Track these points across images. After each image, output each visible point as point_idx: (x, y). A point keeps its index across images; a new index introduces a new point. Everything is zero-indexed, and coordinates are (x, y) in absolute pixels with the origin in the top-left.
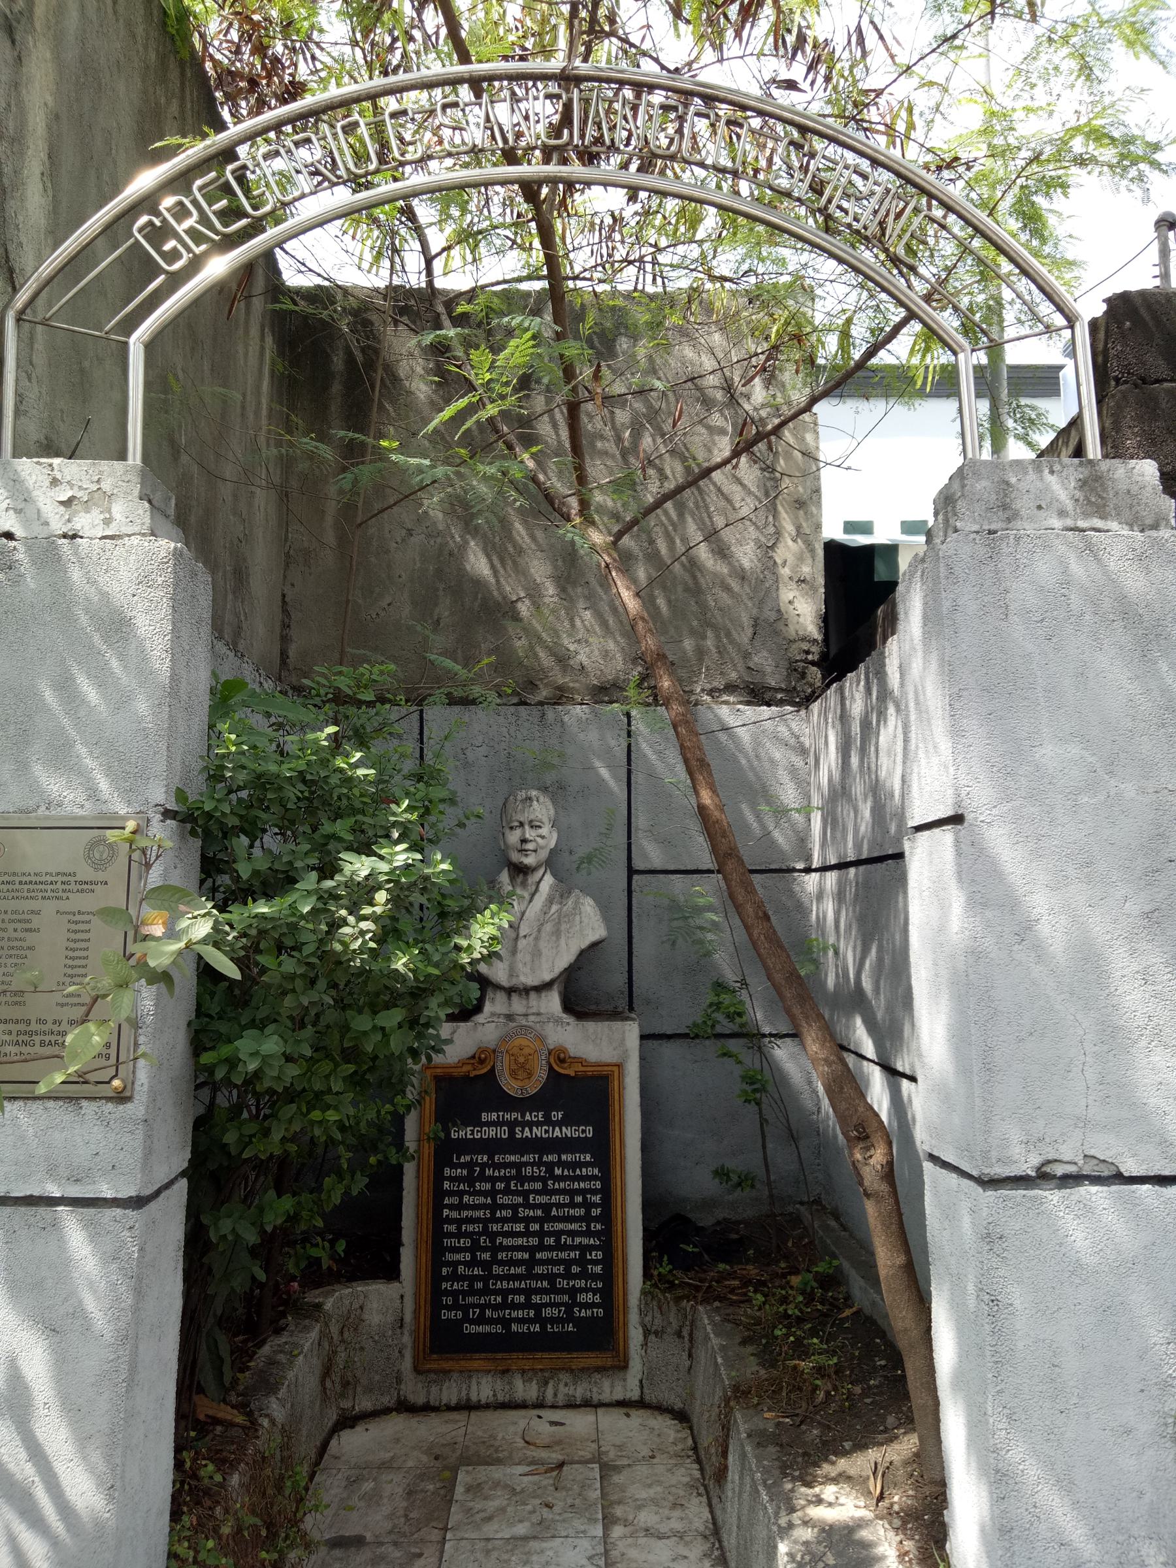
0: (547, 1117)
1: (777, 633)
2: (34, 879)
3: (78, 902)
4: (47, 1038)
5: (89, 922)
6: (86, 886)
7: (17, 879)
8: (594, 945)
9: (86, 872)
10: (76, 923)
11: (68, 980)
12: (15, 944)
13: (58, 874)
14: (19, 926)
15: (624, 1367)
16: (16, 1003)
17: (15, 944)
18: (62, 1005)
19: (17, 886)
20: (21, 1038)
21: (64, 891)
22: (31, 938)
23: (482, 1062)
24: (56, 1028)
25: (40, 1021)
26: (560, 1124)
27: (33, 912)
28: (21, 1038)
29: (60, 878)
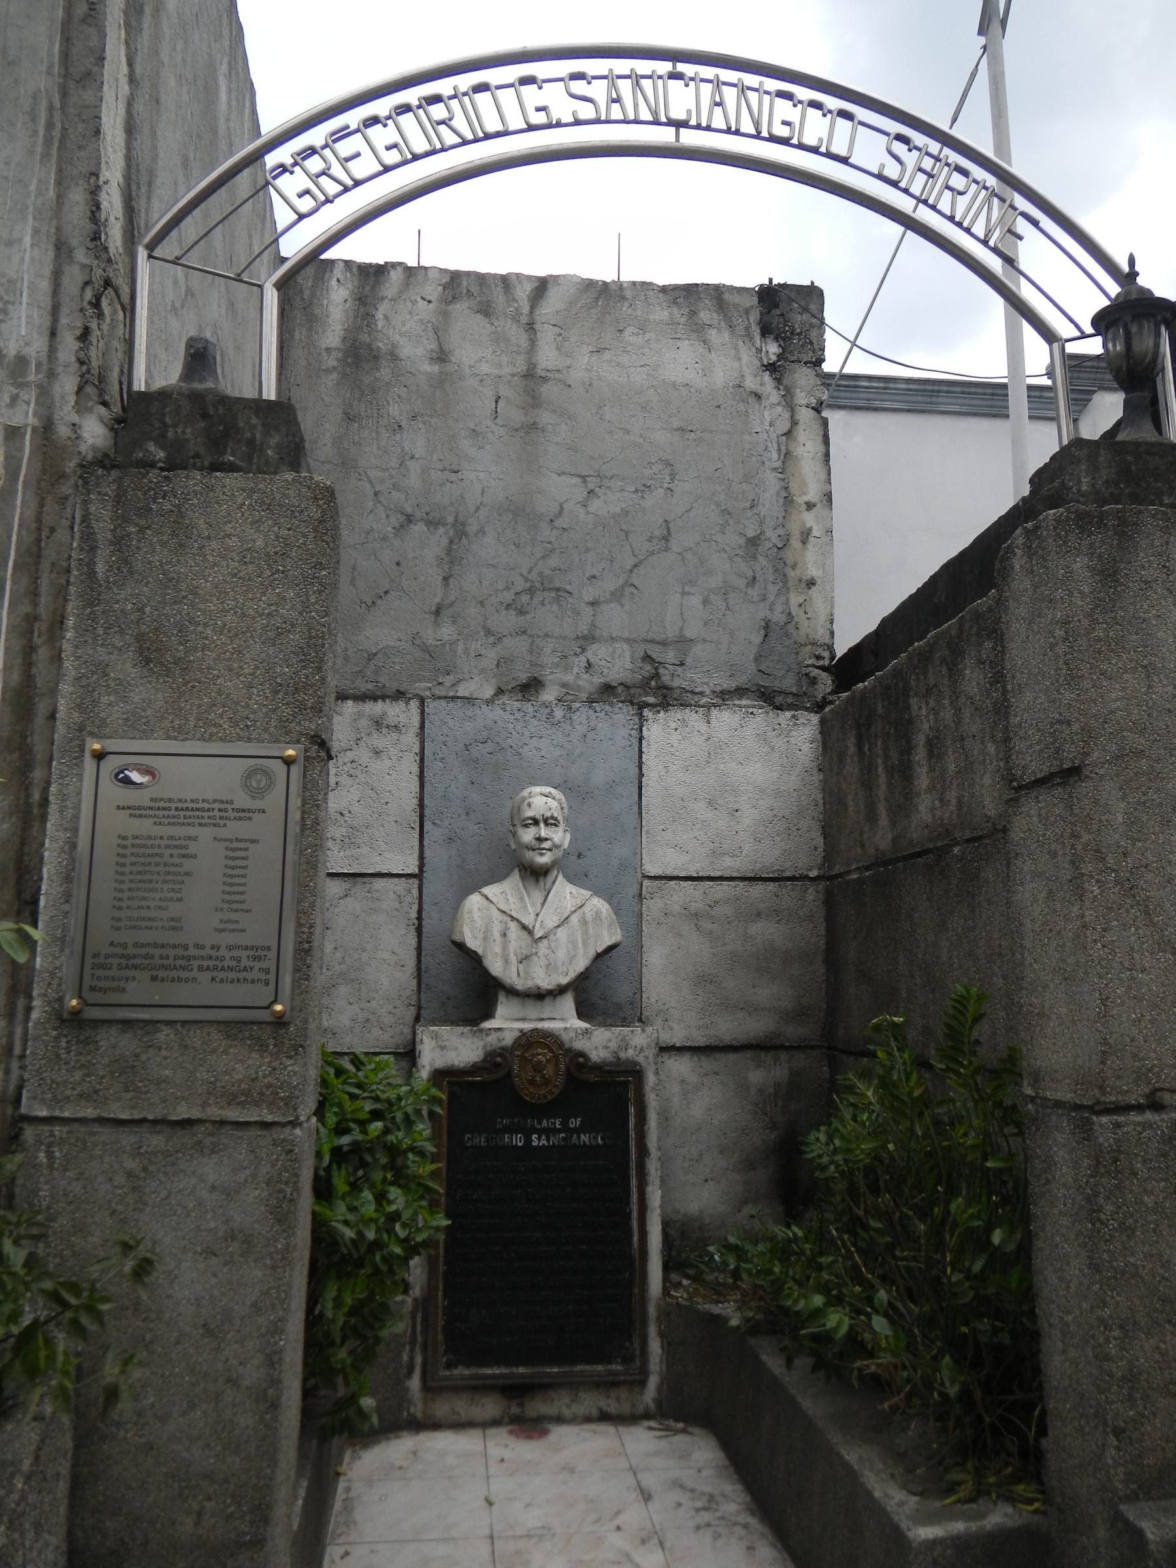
0: (565, 1124)
1: (787, 635)
2: (190, 805)
3: (235, 829)
4: (205, 963)
5: (246, 849)
6: (244, 814)
7: (173, 806)
8: (610, 949)
9: (242, 800)
10: (233, 850)
11: (226, 906)
12: (172, 869)
13: (215, 801)
14: (175, 852)
15: (643, 1383)
16: (174, 928)
17: (172, 869)
18: (221, 931)
19: (173, 813)
20: (178, 962)
21: (221, 818)
22: (188, 864)
23: (497, 1065)
24: (214, 953)
25: (198, 946)
26: (578, 1131)
27: (189, 838)
28: (178, 962)
29: (217, 806)
